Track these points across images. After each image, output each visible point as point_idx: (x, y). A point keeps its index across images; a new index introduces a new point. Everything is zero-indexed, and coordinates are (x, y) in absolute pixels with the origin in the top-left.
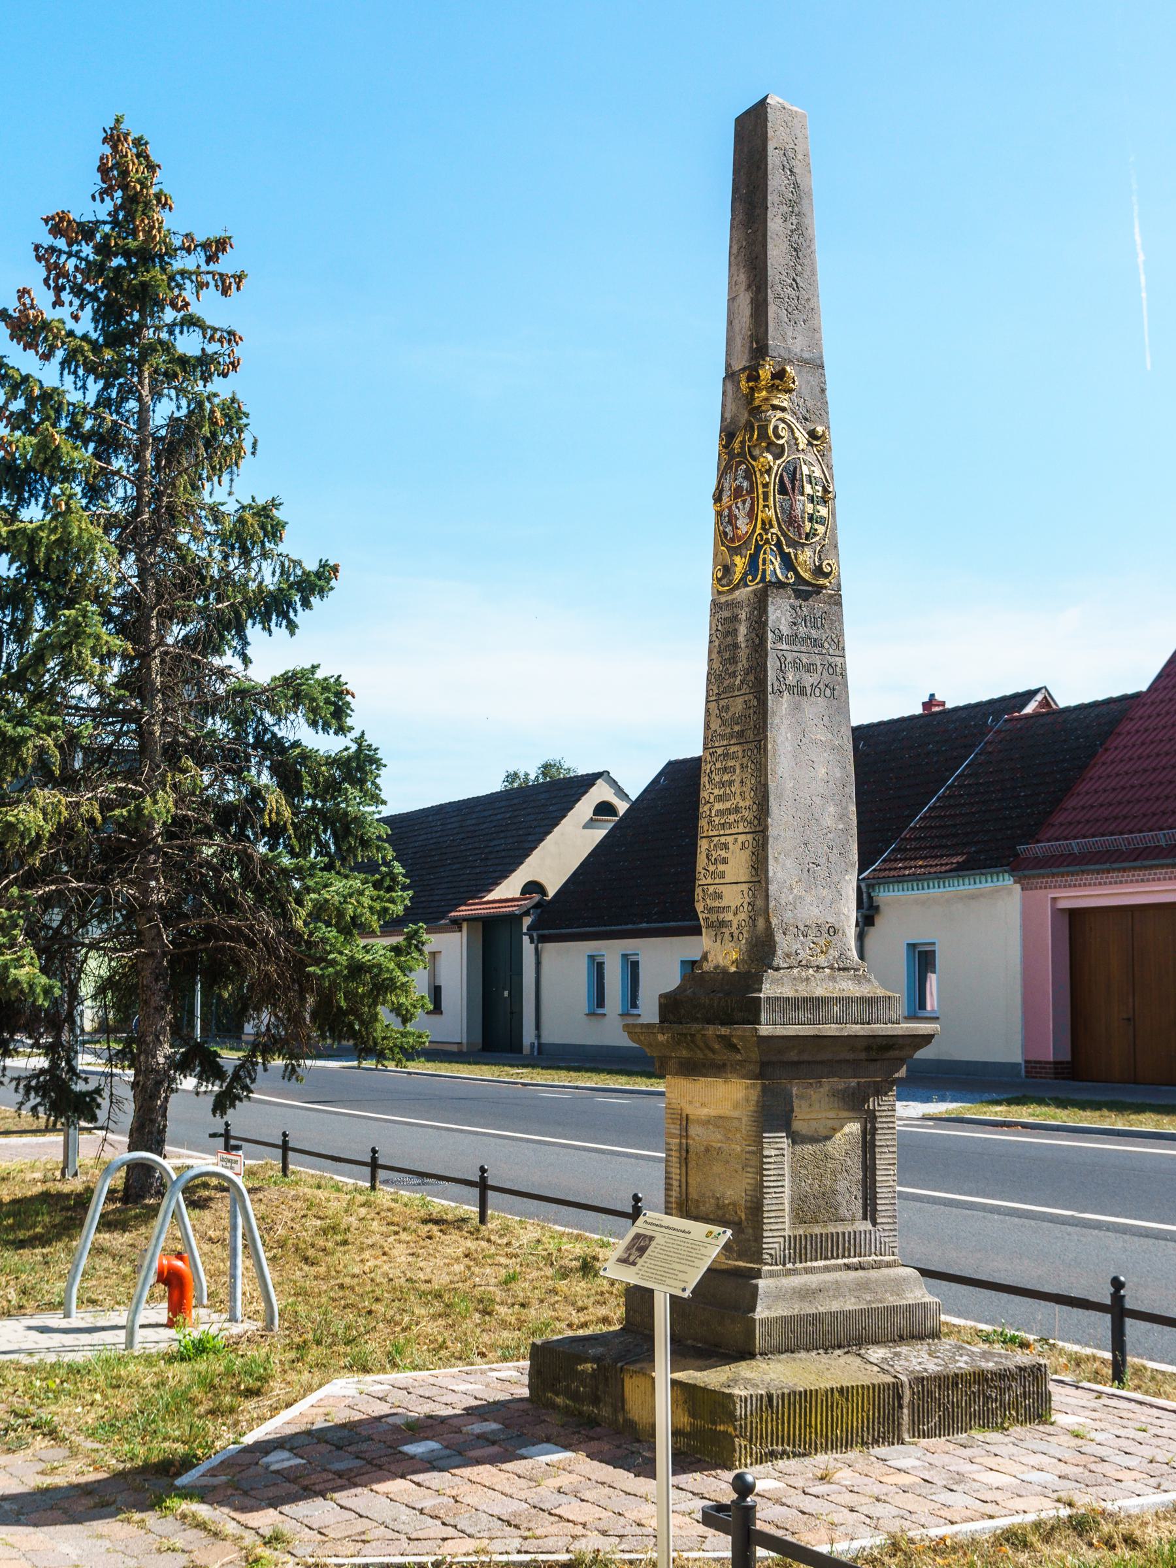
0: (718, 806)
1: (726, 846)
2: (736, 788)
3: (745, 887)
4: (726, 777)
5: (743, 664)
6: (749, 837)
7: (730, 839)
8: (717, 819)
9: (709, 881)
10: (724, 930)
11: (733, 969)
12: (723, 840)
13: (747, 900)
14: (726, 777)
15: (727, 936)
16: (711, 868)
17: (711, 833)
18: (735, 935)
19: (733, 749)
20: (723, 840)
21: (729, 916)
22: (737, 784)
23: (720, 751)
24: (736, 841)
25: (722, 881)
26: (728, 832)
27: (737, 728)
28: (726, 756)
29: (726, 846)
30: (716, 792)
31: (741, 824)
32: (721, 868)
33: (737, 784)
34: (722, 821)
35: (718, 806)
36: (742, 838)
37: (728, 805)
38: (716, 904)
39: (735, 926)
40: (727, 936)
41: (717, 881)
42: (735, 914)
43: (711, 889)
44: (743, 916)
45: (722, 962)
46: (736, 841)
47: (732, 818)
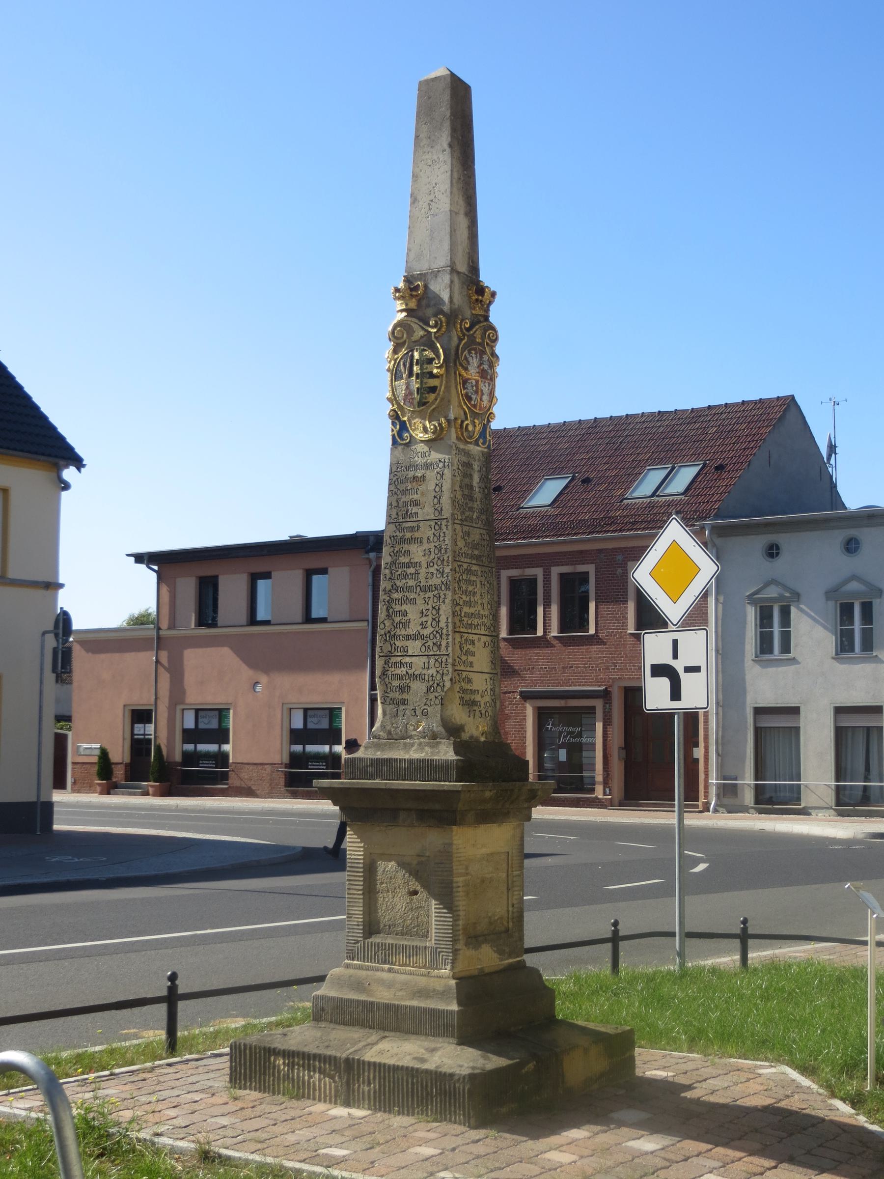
0: (466, 609)
1: (473, 643)
2: (477, 598)
3: (487, 676)
4: (470, 588)
5: (477, 505)
6: (489, 639)
7: (476, 637)
8: (465, 619)
9: (462, 668)
10: (475, 708)
11: (483, 739)
12: (471, 637)
13: (489, 687)
14: (470, 588)
15: (477, 713)
16: (464, 658)
17: (462, 630)
18: (483, 712)
19: (474, 568)
20: (471, 637)
21: (478, 698)
22: (478, 595)
23: (465, 566)
24: (479, 639)
25: (471, 669)
26: (473, 631)
27: (476, 552)
28: (469, 571)
29: (473, 643)
30: (464, 597)
31: (482, 628)
32: (471, 659)
33: (478, 595)
34: (469, 622)
35: (466, 609)
36: (484, 638)
37: (472, 610)
38: (469, 687)
39: (482, 706)
40: (477, 713)
41: (468, 669)
42: (482, 696)
43: (464, 674)
44: (487, 698)
45: (476, 733)
46: (479, 639)
47: (476, 621)
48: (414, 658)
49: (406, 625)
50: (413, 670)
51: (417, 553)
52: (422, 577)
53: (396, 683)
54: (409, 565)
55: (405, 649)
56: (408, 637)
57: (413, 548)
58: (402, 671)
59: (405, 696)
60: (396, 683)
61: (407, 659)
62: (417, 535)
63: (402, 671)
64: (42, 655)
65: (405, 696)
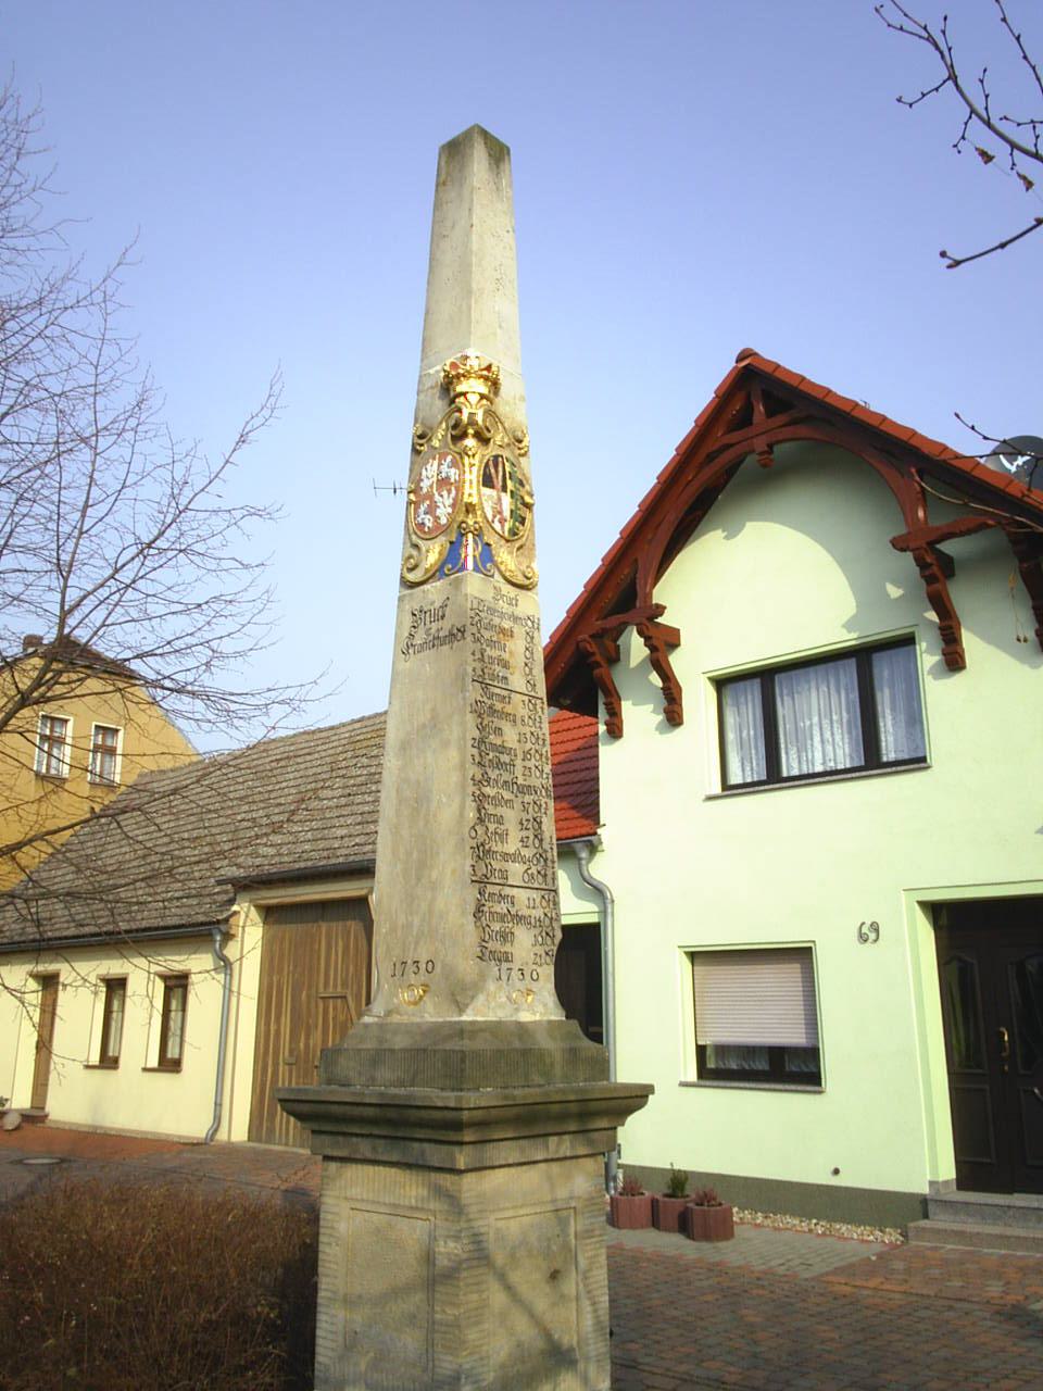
48: (516, 890)
49: (503, 837)
50: (516, 907)
51: (510, 736)
52: (519, 771)
53: (496, 926)
54: (502, 749)
55: (504, 874)
56: (506, 857)
57: (507, 727)
58: (501, 908)
59: (507, 948)
60: (496, 926)
61: (507, 891)
62: (509, 709)
63: (501, 908)
64: (240, 975)
65: (507, 948)
